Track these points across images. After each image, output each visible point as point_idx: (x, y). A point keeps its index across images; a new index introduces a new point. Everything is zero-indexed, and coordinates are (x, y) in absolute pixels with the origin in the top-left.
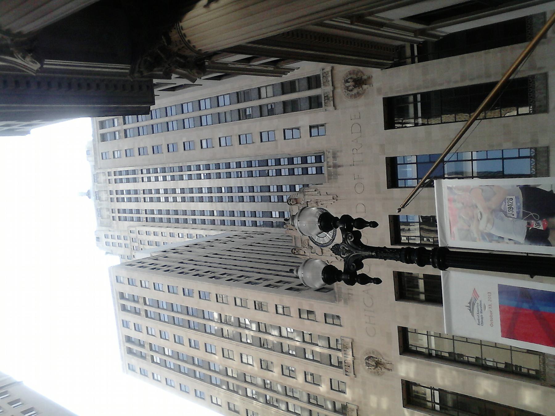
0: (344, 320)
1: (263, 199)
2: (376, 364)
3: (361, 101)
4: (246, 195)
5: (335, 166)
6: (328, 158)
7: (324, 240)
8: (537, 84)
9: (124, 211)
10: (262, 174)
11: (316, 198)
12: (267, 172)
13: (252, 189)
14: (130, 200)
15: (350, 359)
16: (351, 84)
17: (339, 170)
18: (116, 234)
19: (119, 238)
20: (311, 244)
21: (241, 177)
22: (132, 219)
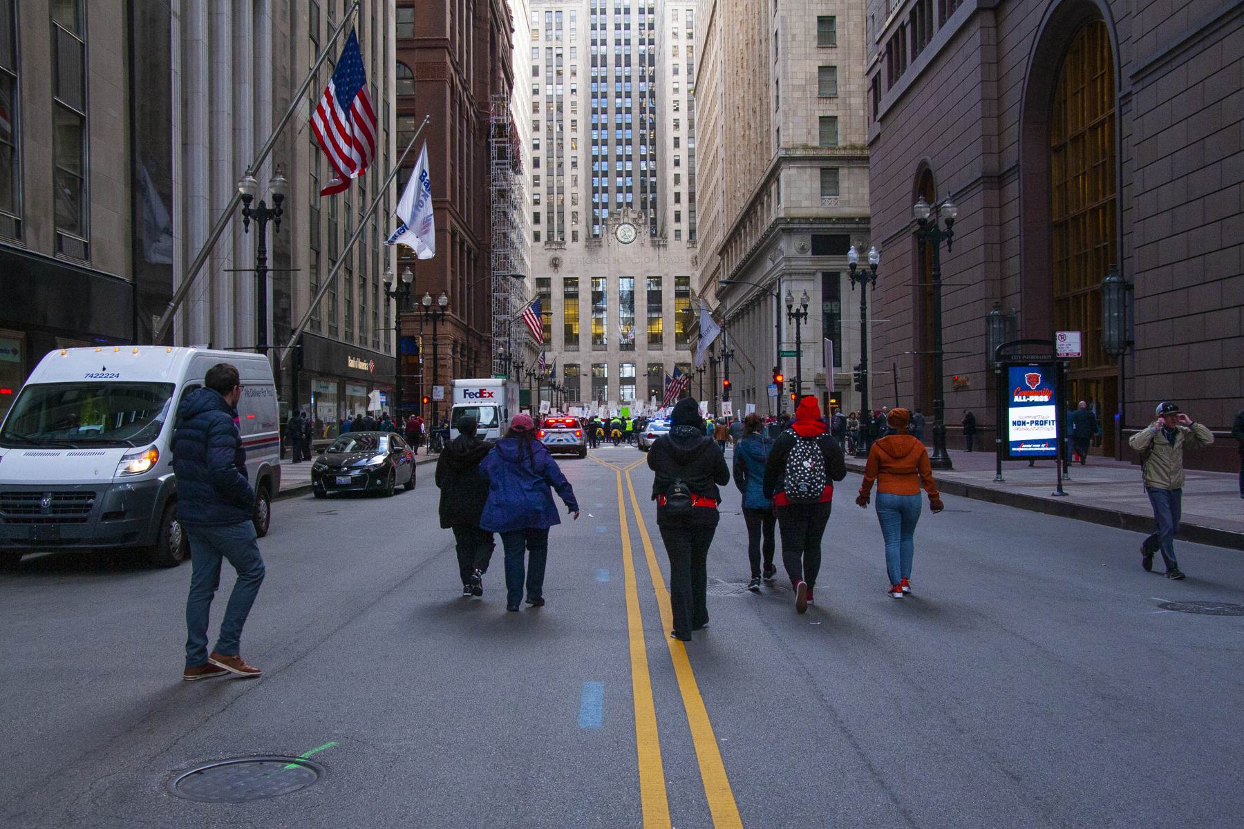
1: (618, 57)
2: (555, 264)
3: (690, 263)
10: (642, 57)
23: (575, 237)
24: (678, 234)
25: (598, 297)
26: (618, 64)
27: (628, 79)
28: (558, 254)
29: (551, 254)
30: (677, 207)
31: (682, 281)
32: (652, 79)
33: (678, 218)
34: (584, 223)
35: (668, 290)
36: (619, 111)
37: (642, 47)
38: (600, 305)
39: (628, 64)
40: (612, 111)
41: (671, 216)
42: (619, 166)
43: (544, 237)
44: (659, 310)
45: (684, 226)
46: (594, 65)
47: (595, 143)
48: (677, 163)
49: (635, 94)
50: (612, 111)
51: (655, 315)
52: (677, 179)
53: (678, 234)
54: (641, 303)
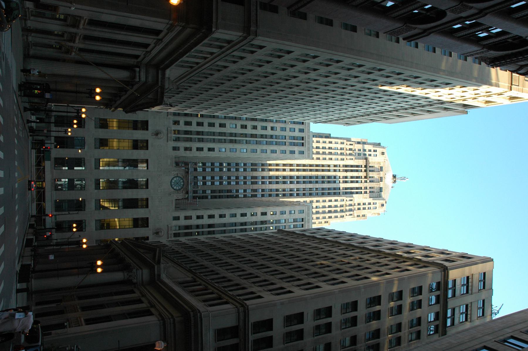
0: (171, 149)
1: (256, 178)
9: (357, 171)
10: (256, 190)
15: (169, 135)
23: (175, 149)
26: (253, 178)
30: (194, 217)
34: (184, 155)
35: (140, 213)
36: (229, 178)
37: (260, 191)
40: (229, 174)
41: (188, 213)
42: (208, 178)
46: (252, 164)
47: (213, 164)
49: (229, 188)
50: (229, 174)
51: (121, 204)
52: (211, 217)
54: (131, 194)
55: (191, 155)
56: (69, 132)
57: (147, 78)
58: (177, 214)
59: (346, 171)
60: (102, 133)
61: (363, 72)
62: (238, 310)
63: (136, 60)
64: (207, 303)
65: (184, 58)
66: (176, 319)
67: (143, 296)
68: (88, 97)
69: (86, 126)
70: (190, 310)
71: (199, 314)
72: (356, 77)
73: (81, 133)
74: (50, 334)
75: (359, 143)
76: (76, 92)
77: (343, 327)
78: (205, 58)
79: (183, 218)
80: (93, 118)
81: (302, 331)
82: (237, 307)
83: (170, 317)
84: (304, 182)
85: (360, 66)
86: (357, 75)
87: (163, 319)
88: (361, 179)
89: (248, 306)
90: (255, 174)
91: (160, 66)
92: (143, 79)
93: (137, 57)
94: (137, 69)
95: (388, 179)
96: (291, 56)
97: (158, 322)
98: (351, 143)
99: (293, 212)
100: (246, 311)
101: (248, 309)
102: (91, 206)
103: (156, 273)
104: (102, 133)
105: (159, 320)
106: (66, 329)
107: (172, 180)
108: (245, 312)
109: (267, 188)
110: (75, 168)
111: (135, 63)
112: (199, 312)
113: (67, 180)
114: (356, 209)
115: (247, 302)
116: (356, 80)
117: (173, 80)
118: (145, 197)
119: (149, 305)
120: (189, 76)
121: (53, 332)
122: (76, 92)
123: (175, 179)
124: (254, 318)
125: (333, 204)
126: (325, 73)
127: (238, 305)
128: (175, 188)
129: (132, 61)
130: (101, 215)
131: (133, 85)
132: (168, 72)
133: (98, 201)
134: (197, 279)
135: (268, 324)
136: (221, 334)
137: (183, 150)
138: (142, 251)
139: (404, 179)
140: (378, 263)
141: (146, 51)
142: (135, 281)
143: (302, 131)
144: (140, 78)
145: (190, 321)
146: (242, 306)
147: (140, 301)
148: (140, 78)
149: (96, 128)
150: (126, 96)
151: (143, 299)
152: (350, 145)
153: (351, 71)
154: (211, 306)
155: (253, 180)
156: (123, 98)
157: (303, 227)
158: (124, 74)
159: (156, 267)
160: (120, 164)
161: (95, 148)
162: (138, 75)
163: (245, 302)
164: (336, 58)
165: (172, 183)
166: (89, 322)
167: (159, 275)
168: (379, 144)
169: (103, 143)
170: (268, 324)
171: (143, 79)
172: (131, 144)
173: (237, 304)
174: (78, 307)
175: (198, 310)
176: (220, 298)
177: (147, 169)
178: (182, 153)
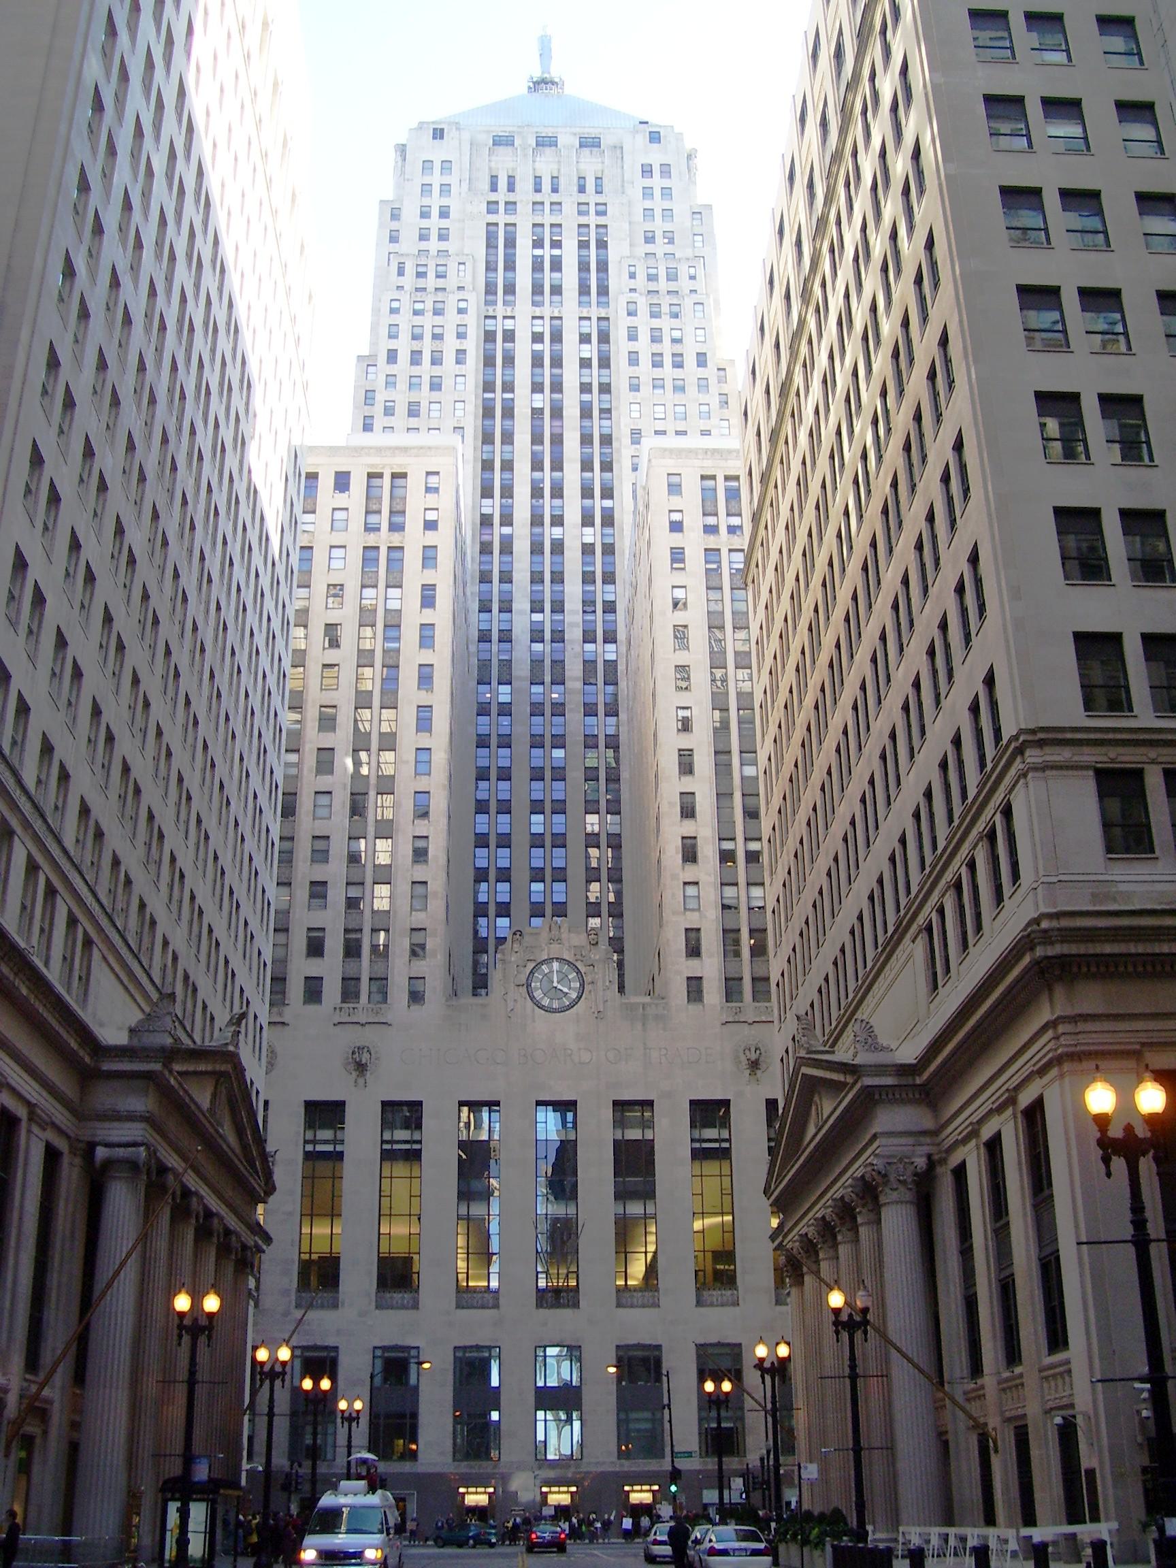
4: (545, 618)
5: (644, 1019)
6: (657, 1005)
7: (537, 989)
8: (729, 1292)
9: (511, 243)
10: (589, 665)
11: (600, 983)
12: (592, 681)
13: (559, 637)
14: (537, 265)
16: (753, 1057)
17: (639, 1026)
18: (453, 203)
19: (444, 214)
20: (531, 965)
21: (584, 612)
22: (490, 267)
24: (695, 987)
25: (475, 1161)
26: (536, 680)
27: (559, 709)
28: (367, 1036)
29: (349, 1038)
31: (709, 1112)
32: (612, 711)
33: (694, 951)
35: (672, 1135)
38: (476, 1185)
39: (559, 680)
40: (521, 774)
43: (332, 990)
44: (648, 1194)
45: (711, 967)
46: (483, 681)
48: (688, 812)
51: (635, 1208)
53: (695, 987)
54: (596, 1171)
55: (441, 928)
56: (350, 1405)
57: (131, 1117)
58: (679, 990)
59: (510, 289)
60: (358, 1279)
61: (93, 255)
62: (1036, 769)
63: (66, 1160)
64: (1007, 889)
65: (53, 974)
66: (1058, 1013)
67: (974, 1134)
68: (210, 1337)
69: (330, 1342)
70: (1026, 960)
71: (1045, 924)
72: (115, 283)
73: (357, 1364)
74: (1091, 1473)
75: (394, 239)
76: (192, 1382)
77: (1123, 349)
78: (51, 892)
79: (694, 962)
80: (298, 1314)
81: (1127, 515)
82: (1025, 775)
83: (1050, 1034)
84: (557, 465)
85: (69, 271)
86: (105, 278)
87: (1058, 1061)
88: (547, 229)
89: (1021, 731)
90: (522, 669)
91: (86, 1060)
92: (133, 1131)
93: (52, 1156)
94: (101, 1153)
95: (543, 115)
96: (34, 556)
97: (1067, 1080)
98: (394, 268)
99: (676, 517)
100: (1044, 738)
101: (1033, 732)
102: (640, 1326)
103: (889, 1081)
104: (358, 1279)
105: (1062, 1076)
106: (1080, 1420)
107: (541, 1007)
108: (1041, 744)
109: (579, 618)
110: (495, 1382)
111: (78, 1161)
112: (1036, 921)
113: (540, 1414)
114: (669, 249)
115: (1008, 732)
116: (125, 279)
117: (140, 1016)
118: (608, 1113)
119: (1009, 1112)
120: (124, 951)
121: (1085, 1463)
122: (192, 1382)
123: (538, 994)
124: (1066, 707)
125: (644, 346)
126: (98, 411)
127: (1018, 765)
128: (574, 995)
129: (71, 1175)
130: (679, 1283)
131: (163, 1169)
132: (113, 1034)
133: (624, 1295)
134: (921, 920)
135: (1097, 648)
136: (1128, 835)
137: (423, 963)
138: (811, 1130)
139: (545, 52)
140: (874, 188)
141: (30, 1119)
142: (921, 1162)
143: (342, 482)
144: (135, 1144)
145: (1062, 959)
146: (1020, 751)
147: (994, 1146)
148: (135, 1144)
149: (335, 1305)
150: (204, 1191)
151: (987, 1133)
152: (401, 272)
153: (92, 306)
154: (1016, 876)
155: (548, 679)
156: (214, 1204)
157: (737, 478)
158: (122, 1202)
159: (868, 1081)
160: (477, 1209)
161: (415, 1306)
162: (121, 1152)
163: (1004, 742)
164: (39, 373)
165: (555, 1005)
166: (1057, 1338)
167: (904, 1070)
168: (402, 150)
169: (396, 1276)
170: (1097, 648)
171: (133, 1131)
172: (400, 1169)
173: (1012, 772)
174: (1006, 1374)
175: (1029, 924)
176: (991, 836)
177: (493, 1104)
178: (432, 968)
